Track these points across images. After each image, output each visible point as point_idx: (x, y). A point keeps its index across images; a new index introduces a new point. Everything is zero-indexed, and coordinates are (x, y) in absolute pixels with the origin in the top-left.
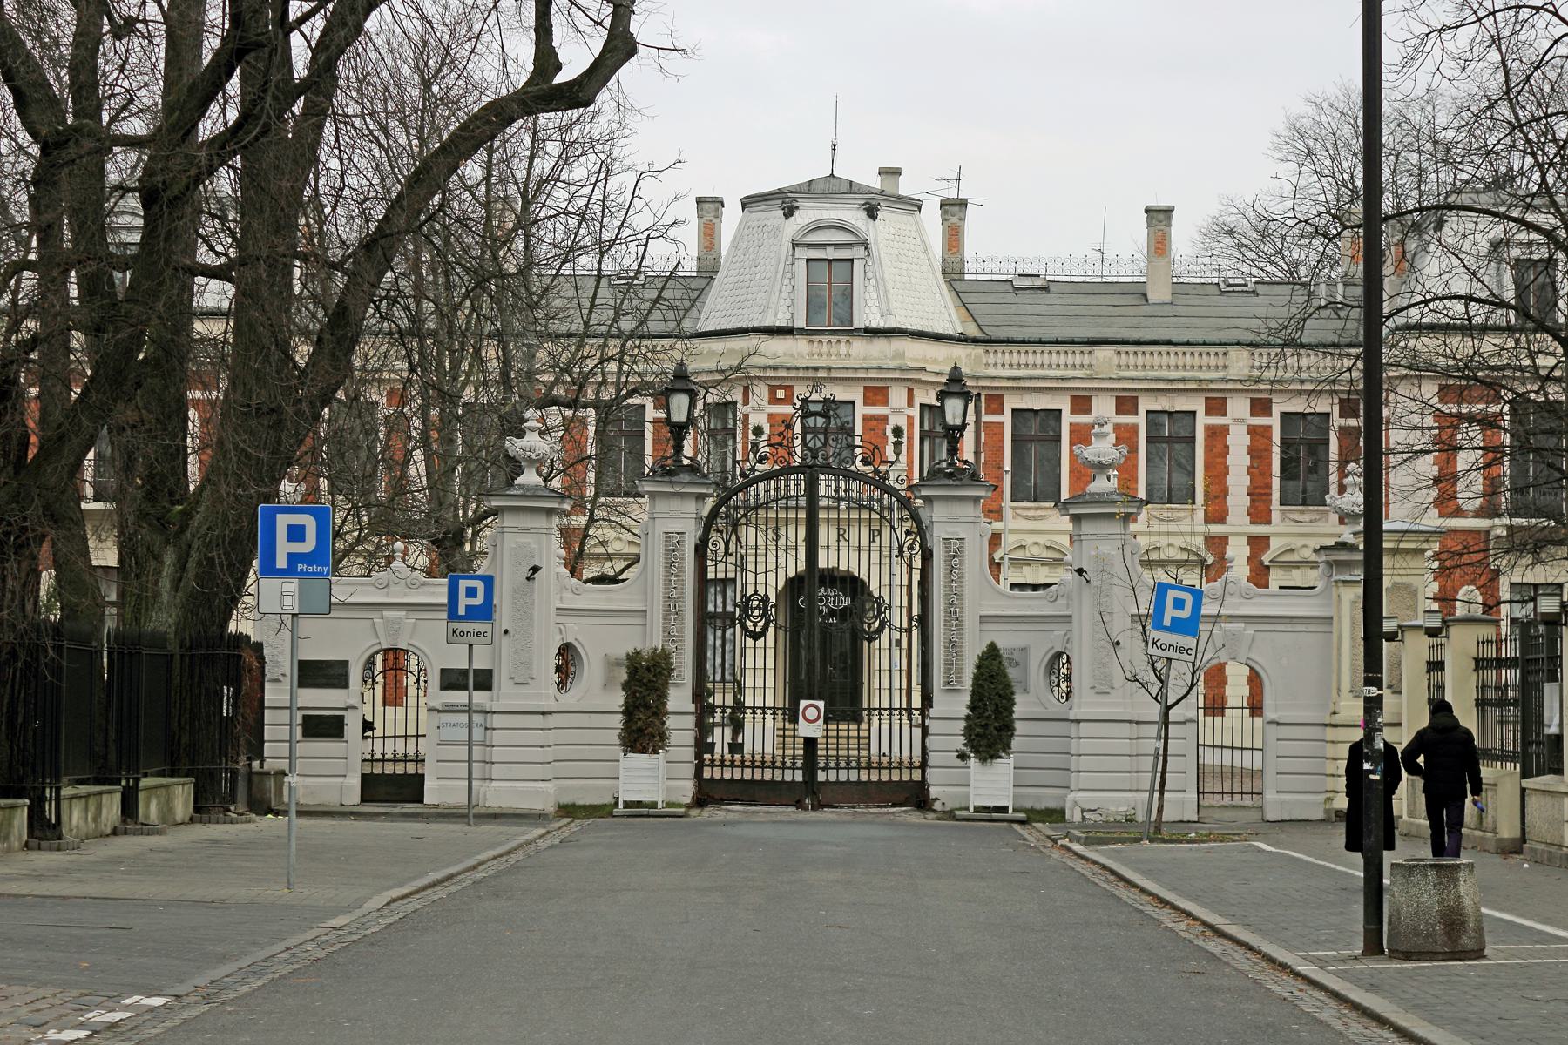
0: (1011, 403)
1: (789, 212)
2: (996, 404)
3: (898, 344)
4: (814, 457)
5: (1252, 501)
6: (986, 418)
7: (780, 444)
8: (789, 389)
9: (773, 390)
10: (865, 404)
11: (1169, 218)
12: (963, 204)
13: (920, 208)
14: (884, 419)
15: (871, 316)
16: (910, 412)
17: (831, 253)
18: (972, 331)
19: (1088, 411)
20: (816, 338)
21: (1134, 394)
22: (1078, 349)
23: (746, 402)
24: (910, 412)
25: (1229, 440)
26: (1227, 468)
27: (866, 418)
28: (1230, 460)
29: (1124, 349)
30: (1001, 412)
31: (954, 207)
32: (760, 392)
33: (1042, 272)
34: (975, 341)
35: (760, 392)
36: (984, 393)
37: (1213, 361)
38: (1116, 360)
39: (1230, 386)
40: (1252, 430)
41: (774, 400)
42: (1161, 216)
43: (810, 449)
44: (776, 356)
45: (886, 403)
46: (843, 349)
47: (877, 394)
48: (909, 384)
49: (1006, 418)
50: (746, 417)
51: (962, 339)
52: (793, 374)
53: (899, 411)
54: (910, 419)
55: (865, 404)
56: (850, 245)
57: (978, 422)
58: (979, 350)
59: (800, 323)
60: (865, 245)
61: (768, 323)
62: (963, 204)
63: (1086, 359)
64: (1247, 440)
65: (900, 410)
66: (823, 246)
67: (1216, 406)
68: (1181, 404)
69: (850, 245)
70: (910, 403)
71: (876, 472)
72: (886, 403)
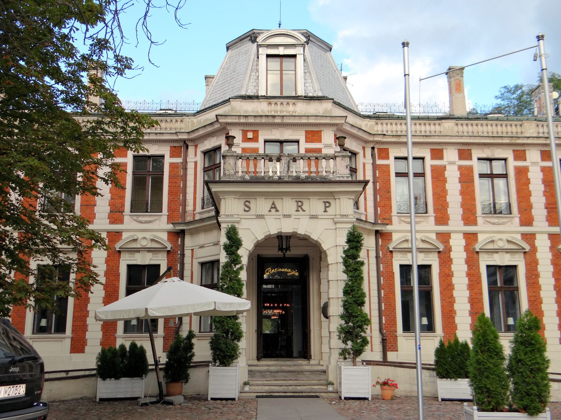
2: (384, 154)
5: (548, 212)
6: (379, 162)
8: (256, 132)
9: (245, 133)
10: (307, 141)
11: (462, 73)
13: (331, 50)
15: (308, 91)
17: (281, 51)
19: (441, 158)
20: (273, 101)
21: (469, 148)
22: (432, 122)
25: (530, 175)
26: (530, 192)
28: (531, 187)
29: (460, 122)
30: (387, 158)
33: (389, 111)
36: (377, 147)
37: (514, 129)
38: (456, 128)
39: (530, 141)
40: (543, 169)
41: (246, 139)
42: (458, 72)
44: (246, 111)
45: (320, 141)
46: (291, 108)
48: (335, 128)
52: (258, 120)
55: (307, 141)
56: (293, 46)
57: (374, 164)
59: (262, 93)
61: (243, 93)
63: (438, 128)
64: (541, 175)
66: (277, 46)
67: (520, 155)
68: (499, 153)
69: (293, 46)
72: (320, 141)
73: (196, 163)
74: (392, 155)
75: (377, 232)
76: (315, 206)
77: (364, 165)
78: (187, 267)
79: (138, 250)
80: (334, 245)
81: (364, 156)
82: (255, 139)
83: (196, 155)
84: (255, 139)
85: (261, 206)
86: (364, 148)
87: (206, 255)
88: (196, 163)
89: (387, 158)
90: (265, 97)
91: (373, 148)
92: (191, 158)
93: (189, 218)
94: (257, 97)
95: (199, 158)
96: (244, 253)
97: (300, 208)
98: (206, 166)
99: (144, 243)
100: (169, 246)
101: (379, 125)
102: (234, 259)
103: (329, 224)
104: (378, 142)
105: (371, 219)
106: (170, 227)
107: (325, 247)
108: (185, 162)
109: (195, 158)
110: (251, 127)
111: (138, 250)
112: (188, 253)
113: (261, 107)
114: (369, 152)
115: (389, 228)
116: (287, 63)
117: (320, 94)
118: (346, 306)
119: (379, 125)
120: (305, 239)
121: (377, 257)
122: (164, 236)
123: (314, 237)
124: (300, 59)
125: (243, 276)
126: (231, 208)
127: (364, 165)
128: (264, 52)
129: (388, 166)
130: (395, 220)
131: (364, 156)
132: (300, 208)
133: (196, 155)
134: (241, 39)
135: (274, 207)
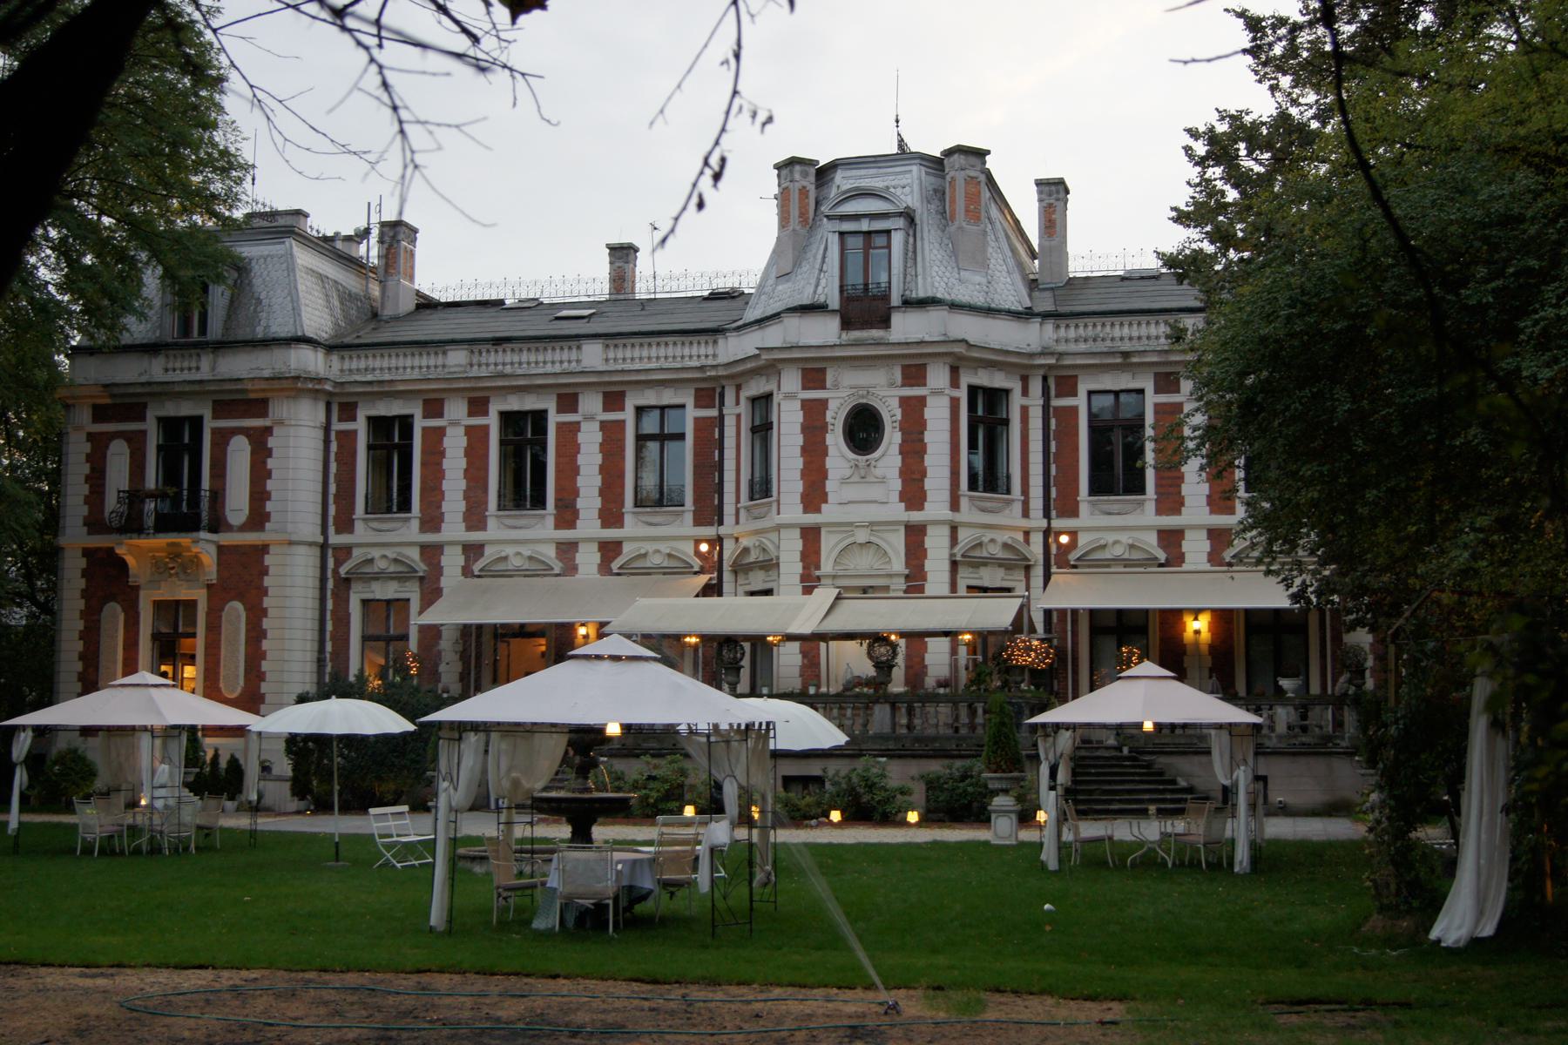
16: (956, 393)
17: (865, 226)
24: (956, 393)
49: (1080, 401)
54: (955, 403)
57: (1046, 408)
66: (856, 217)
70: (955, 383)
73: (739, 416)
74: (1083, 389)
77: (1025, 410)
81: (1025, 393)
83: (738, 403)
86: (1025, 380)
88: (739, 416)
91: (1045, 379)
92: (730, 410)
95: (744, 408)
98: (757, 423)
101: (1063, 330)
104: (1050, 367)
108: (721, 417)
109: (736, 412)
114: (1036, 387)
116: (880, 241)
119: (1063, 330)
127: (1025, 410)
129: (1074, 410)
131: (1025, 393)
133: (738, 403)
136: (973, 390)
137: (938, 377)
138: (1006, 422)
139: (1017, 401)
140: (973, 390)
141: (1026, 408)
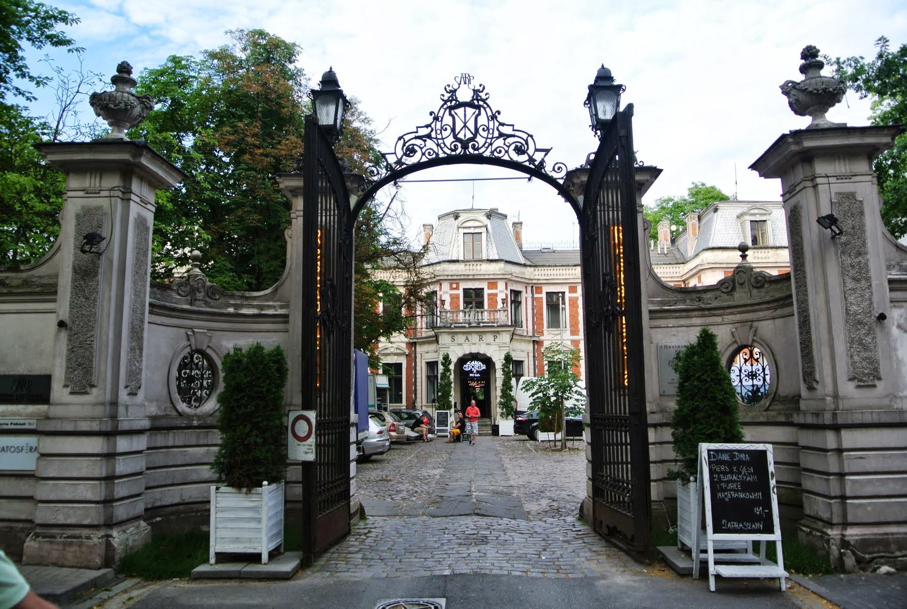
0: (546, 289)
1: (457, 217)
2: (539, 290)
3: (501, 265)
4: (465, 146)
6: (536, 296)
7: (429, 136)
8: (458, 284)
9: (451, 284)
12: (521, 223)
13: (506, 216)
14: (496, 295)
17: (472, 230)
18: (528, 263)
23: (441, 290)
27: (489, 295)
30: (541, 292)
31: (517, 225)
32: (446, 286)
34: (530, 266)
35: (446, 286)
41: (452, 289)
43: (460, 140)
47: (493, 284)
49: (544, 296)
50: (441, 296)
51: (525, 265)
53: (501, 292)
54: (507, 295)
57: (533, 297)
58: (532, 269)
59: (461, 258)
60: (486, 226)
61: (450, 258)
62: (521, 223)
65: (502, 291)
71: (531, 160)
75: (534, 341)
76: (489, 338)
78: (418, 364)
79: (388, 355)
80: (499, 361)
82: (457, 288)
84: (457, 288)
85: (461, 338)
87: (431, 357)
89: (541, 292)
90: (463, 261)
93: (419, 335)
94: (458, 261)
96: (452, 367)
97: (481, 339)
99: (392, 350)
100: (407, 352)
102: (447, 370)
103: (496, 347)
105: (530, 334)
106: (407, 340)
107: (494, 360)
110: (454, 281)
111: (388, 355)
112: (418, 356)
113: (459, 269)
114: (529, 289)
115: (542, 338)
117: (497, 258)
118: (502, 391)
120: (485, 355)
121: (534, 357)
122: (404, 346)
123: (489, 355)
124: (484, 235)
125: (452, 377)
126: (444, 339)
128: (462, 231)
130: (545, 333)
132: (481, 339)
134: (447, 215)
135: (467, 339)
136: (511, 291)
137: (501, 285)
138: (520, 303)
139: (524, 295)
140: (511, 291)
141: (526, 297)
